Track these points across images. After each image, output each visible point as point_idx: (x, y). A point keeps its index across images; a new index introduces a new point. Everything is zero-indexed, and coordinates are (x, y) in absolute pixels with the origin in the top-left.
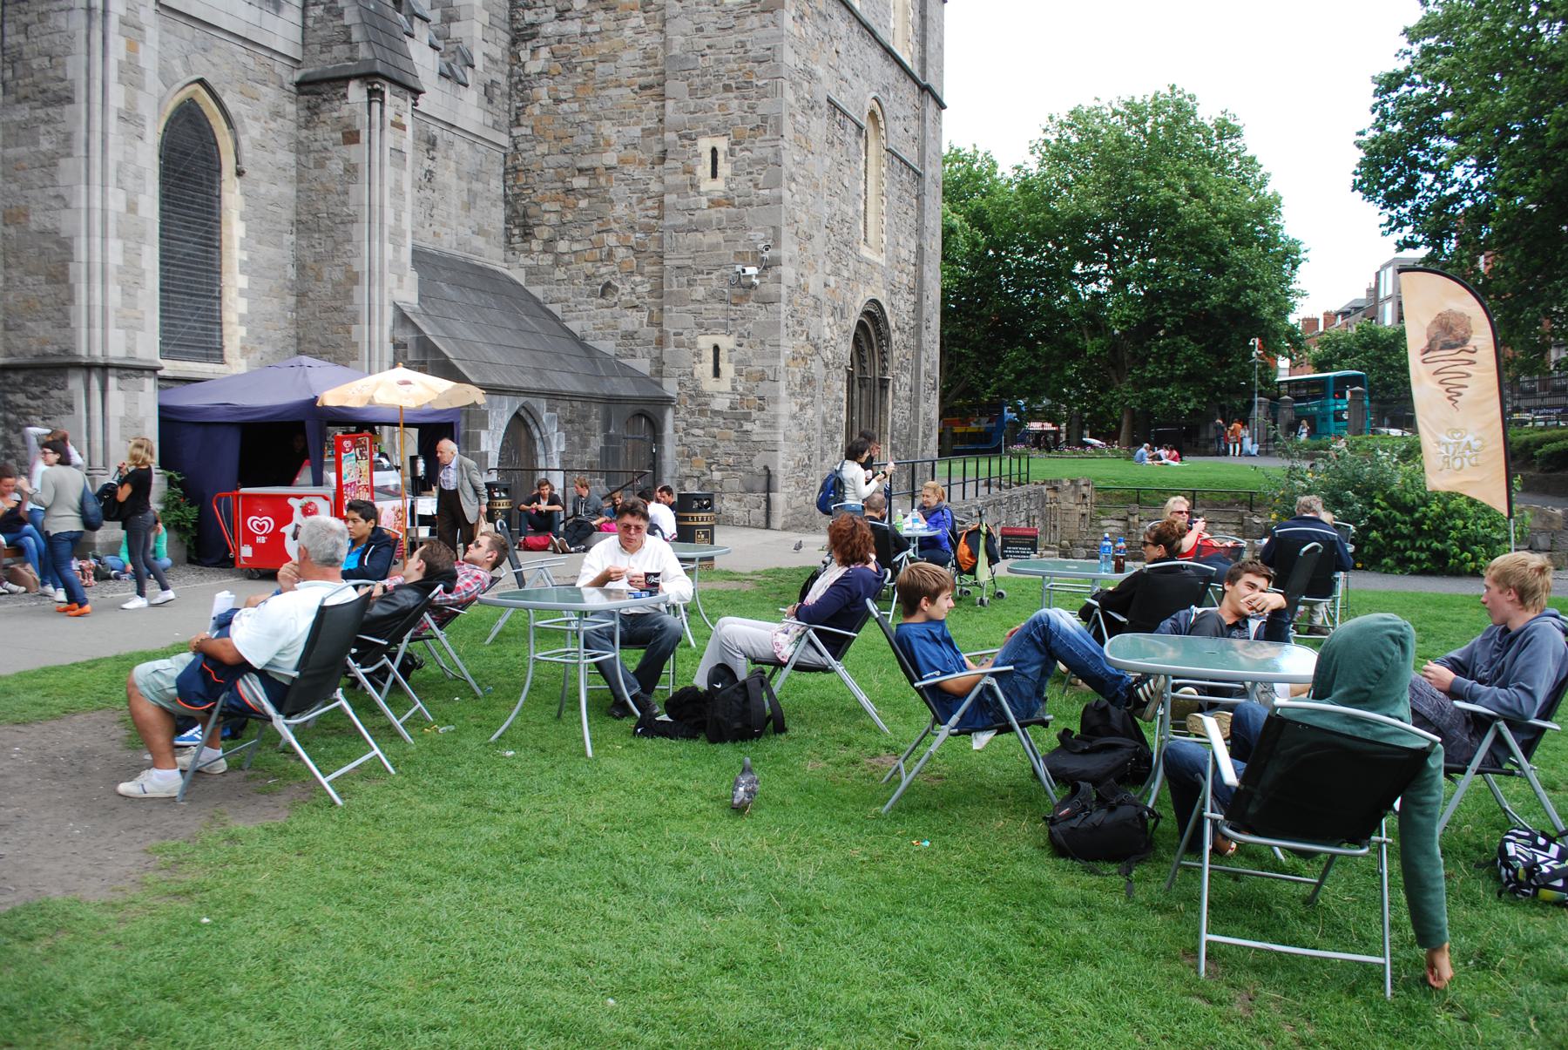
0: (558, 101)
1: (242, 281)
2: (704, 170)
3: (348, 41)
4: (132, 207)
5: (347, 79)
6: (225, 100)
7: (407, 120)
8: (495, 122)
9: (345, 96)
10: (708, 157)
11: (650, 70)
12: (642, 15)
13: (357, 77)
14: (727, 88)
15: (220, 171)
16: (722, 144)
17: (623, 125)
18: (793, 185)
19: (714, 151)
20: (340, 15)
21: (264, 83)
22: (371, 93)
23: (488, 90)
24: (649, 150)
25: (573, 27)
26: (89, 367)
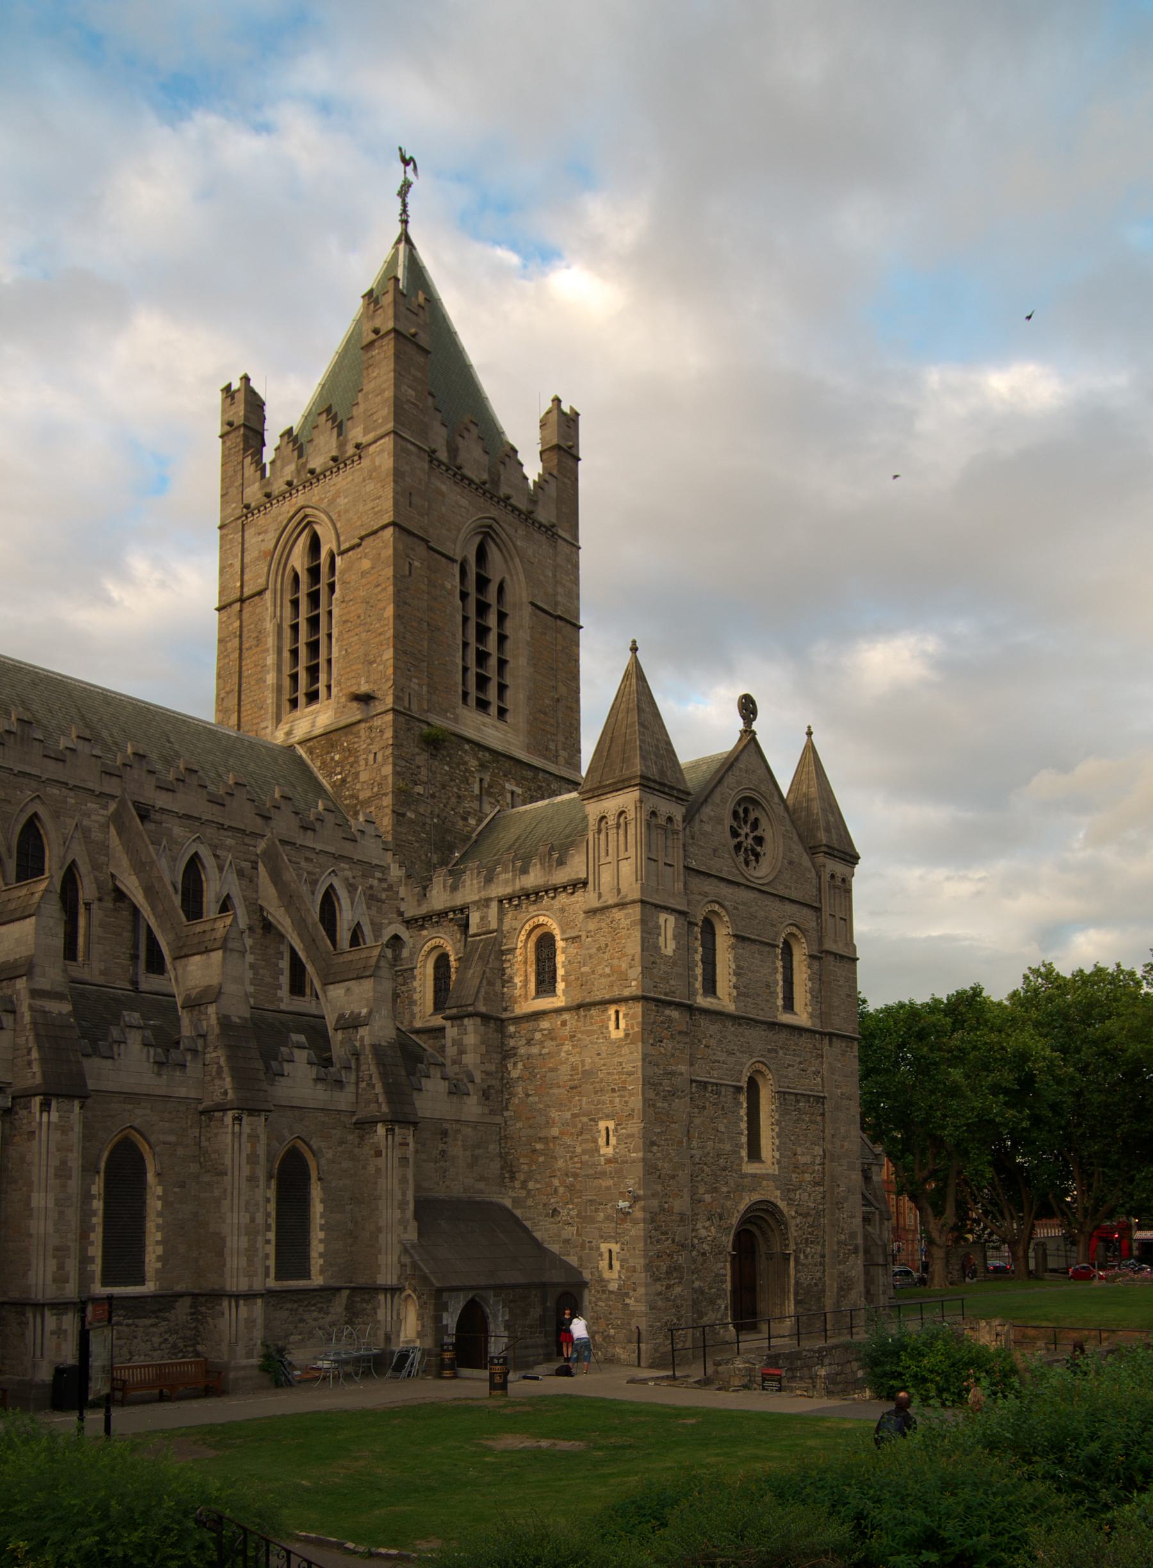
0: (528, 1095)
2: (602, 1141)
3: (377, 1102)
5: (377, 1122)
6: (312, 1143)
7: (410, 1140)
8: (491, 1110)
9: (376, 1131)
10: (604, 1133)
11: (575, 1077)
12: (571, 1043)
13: (381, 1122)
14: (613, 1090)
15: (309, 1179)
16: (611, 1125)
17: (560, 1111)
19: (607, 1129)
20: (374, 1087)
21: (334, 1128)
22: (387, 1130)
23: (486, 1094)
24: (575, 1126)
25: (535, 1050)
26: (230, 1296)
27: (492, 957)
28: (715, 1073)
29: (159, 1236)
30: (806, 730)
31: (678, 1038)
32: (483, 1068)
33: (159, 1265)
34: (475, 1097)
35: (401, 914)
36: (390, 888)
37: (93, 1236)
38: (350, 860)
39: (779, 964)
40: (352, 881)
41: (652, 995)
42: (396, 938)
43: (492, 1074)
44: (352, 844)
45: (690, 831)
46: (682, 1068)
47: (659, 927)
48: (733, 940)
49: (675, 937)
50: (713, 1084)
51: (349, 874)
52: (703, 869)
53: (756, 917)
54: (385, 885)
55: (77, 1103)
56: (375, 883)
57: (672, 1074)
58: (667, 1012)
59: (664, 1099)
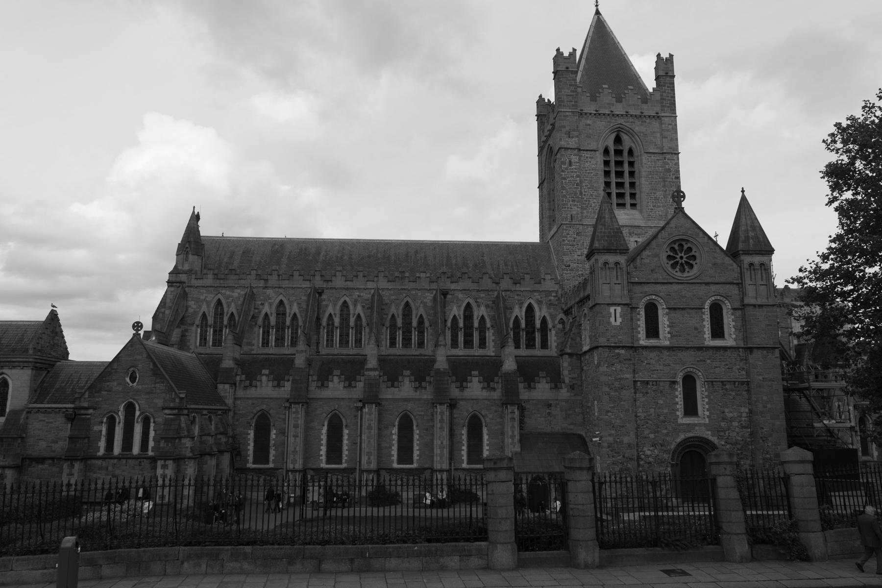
1: (487, 448)
4: (442, 443)
7: (516, 410)
18: (610, 414)
23: (572, 387)
27: (574, 328)
28: (655, 376)
29: (418, 448)
30: (741, 190)
31: (625, 362)
32: (570, 376)
33: (418, 458)
34: (566, 389)
35: (563, 309)
36: (559, 298)
37: (393, 448)
38: (539, 291)
39: (707, 317)
40: (540, 299)
41: (606, 344)
42: (561, 319)
43: (575, 378)
44: (539, 285)
45: (634, 265)
46: (628, 376)
47: (611, 313)
48: (667, 311)
49: (621, 316)
50: (653, 381)
51: (539, 297)
52: (644, 280)
53: (686, 297)
54: (557, 298)
55: (374, 405)
56: (552, 298)
57: (621, 379)
58: (617, 351)
59: (616, 391)
